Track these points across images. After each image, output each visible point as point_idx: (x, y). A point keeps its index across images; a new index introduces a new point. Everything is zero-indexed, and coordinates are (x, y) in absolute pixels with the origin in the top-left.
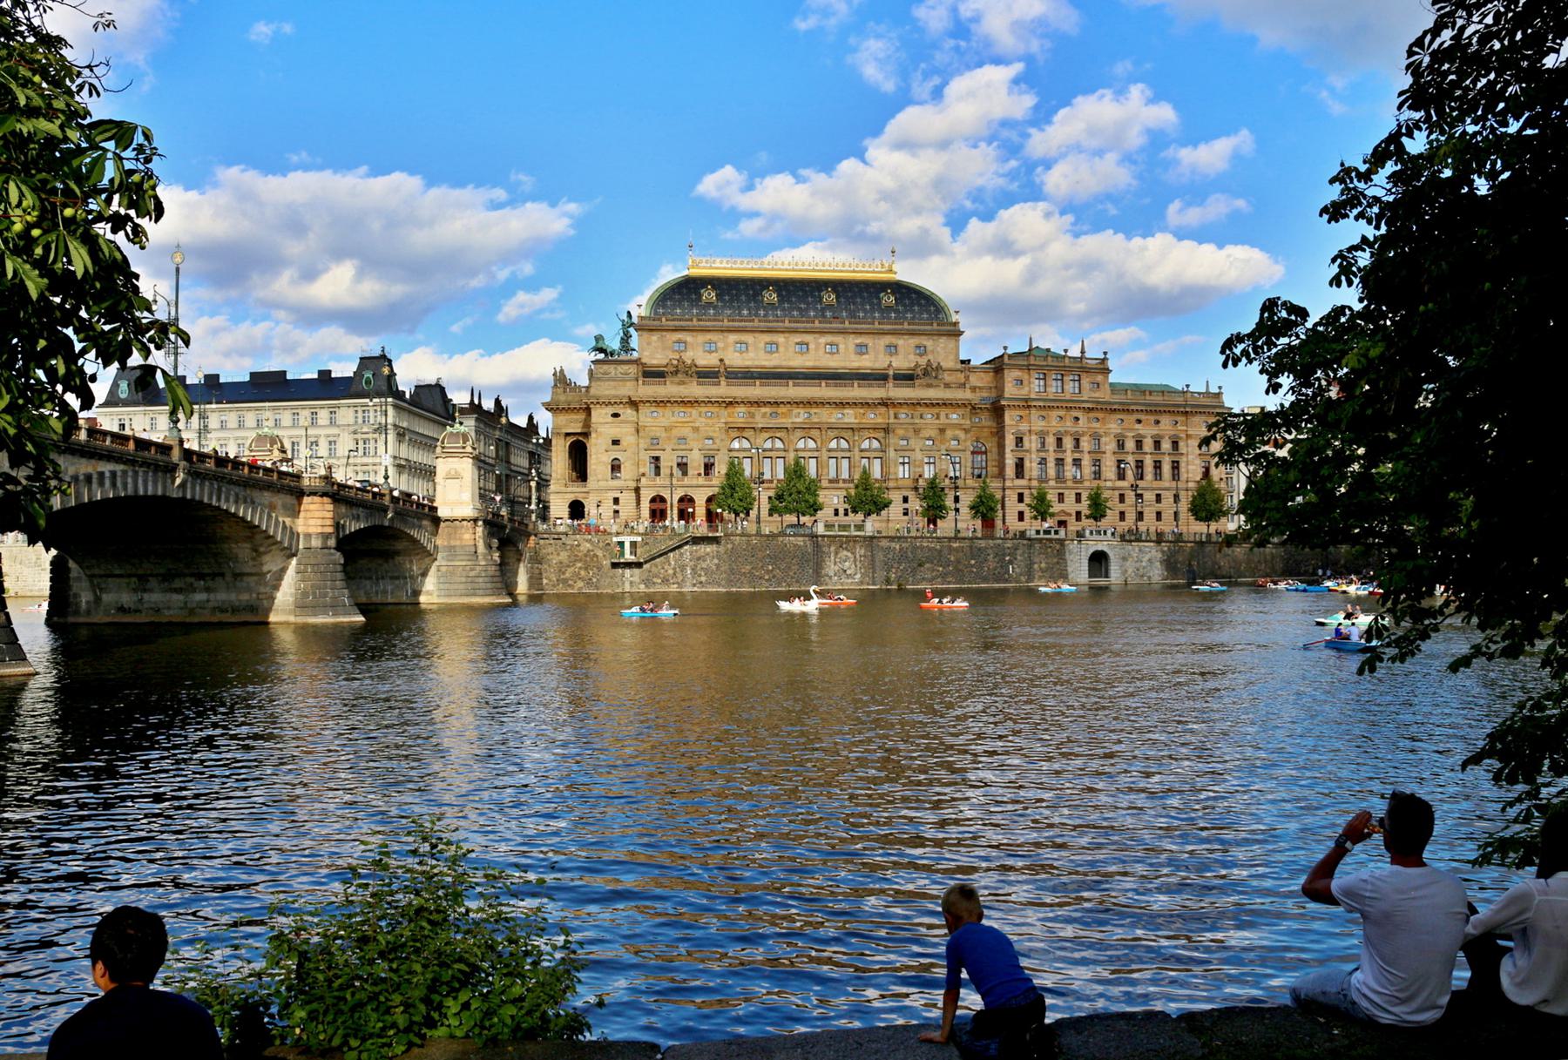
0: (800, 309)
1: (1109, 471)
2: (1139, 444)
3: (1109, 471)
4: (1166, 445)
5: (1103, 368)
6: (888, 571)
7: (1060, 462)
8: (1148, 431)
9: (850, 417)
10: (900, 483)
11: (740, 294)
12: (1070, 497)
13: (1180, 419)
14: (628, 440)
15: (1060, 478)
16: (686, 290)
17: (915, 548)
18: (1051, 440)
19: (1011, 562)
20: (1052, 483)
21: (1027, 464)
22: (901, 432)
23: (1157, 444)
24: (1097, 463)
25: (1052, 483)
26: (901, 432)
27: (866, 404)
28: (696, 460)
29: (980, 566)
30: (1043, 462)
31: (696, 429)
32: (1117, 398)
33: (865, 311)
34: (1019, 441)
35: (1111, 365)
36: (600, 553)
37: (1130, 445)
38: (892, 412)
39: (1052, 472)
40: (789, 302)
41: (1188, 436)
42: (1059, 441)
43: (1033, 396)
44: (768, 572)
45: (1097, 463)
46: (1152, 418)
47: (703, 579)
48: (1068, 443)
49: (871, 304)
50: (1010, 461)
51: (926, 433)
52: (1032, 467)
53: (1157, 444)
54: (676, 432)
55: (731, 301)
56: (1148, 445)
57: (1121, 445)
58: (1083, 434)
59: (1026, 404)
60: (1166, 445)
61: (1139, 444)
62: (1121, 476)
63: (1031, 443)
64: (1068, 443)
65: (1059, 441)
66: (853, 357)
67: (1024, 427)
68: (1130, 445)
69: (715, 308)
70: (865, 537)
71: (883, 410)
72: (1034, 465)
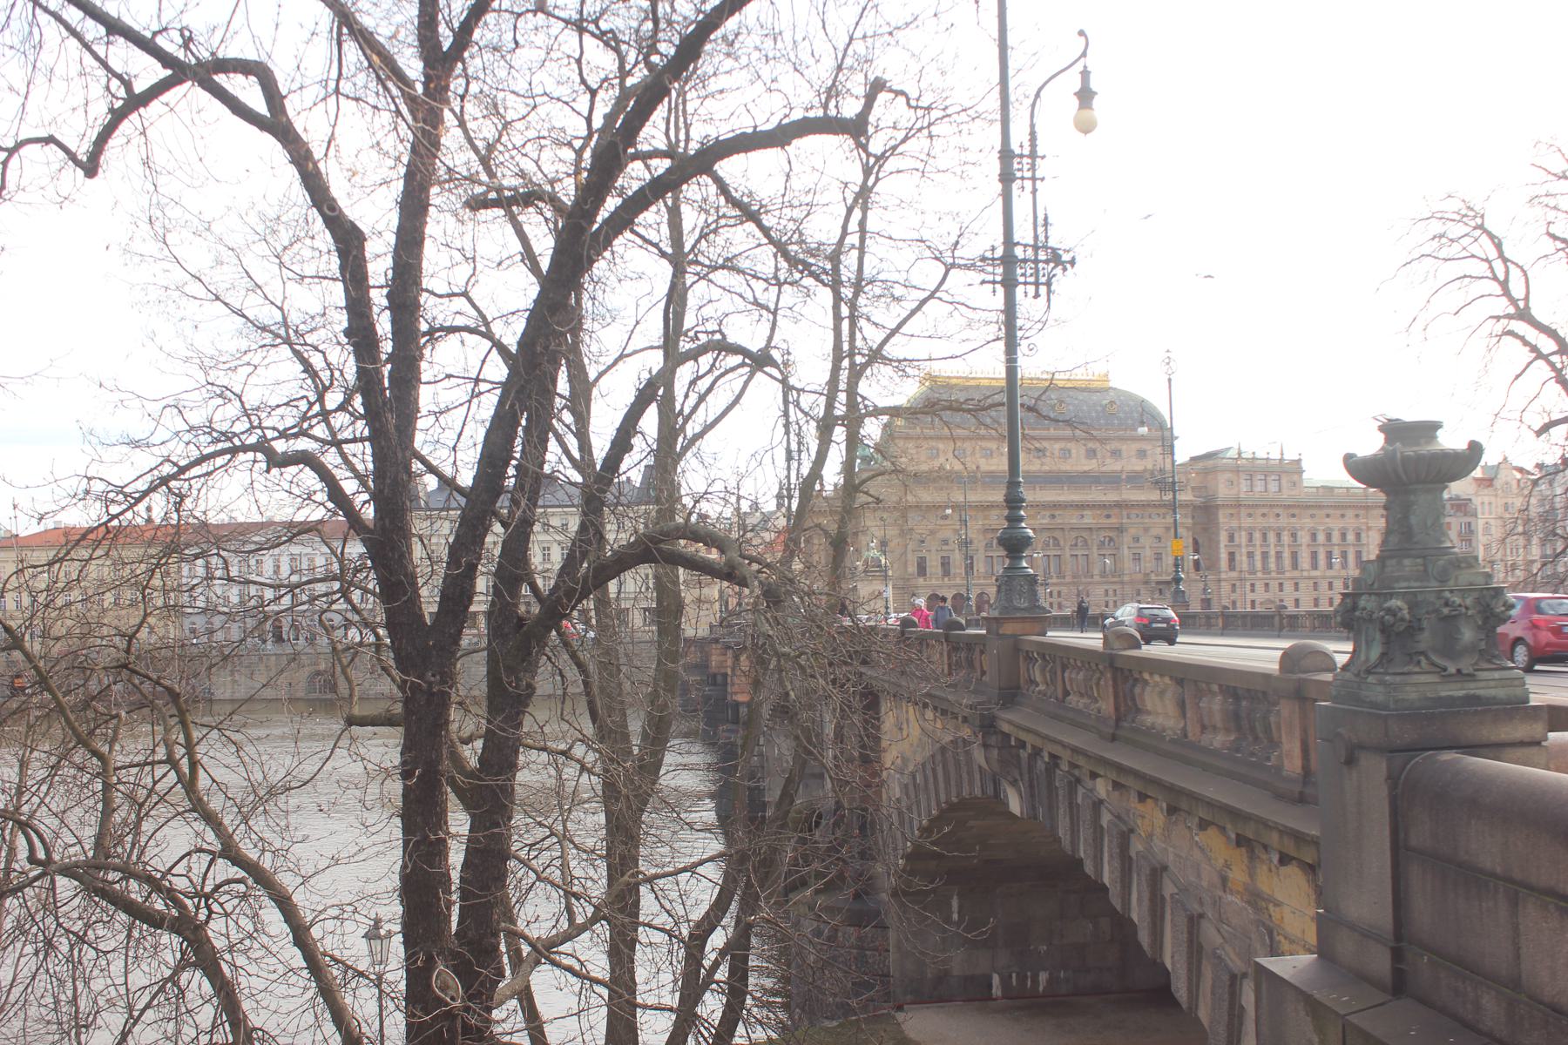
1: (1305, 562)
2: (1329, 537)
3: (1305, 562)
4: (1351, 537)
5: (1296, 468)
7: (1265, 555)
8: (1335, 524)
9: (1089, 519)
12: (1274, 585)
13: (1361, 512)
15: (1265, 569)
18: (1257, 535)
20: (1259, 575)
21: (1237, 557)
22: (1133, 531)
23: (1343, 536)
24: (1294, 556)
25: (1259, 575)
26: (1133, 531)
27: (1103, 506)
30: (1250, 555)
34: (1231, 538)
35: (1304, 465)
37: (1321, 538)
38: (1125, 513)
39: (1259, 565)
41: (1369, 529)
42: (1265, 536)
46: (1339, 512)
48: (1272, 537)
50: (1224, 556)
51: (1154, 532)
52: (1242, 560)
53: (1343, 536)
56: (1336, 538)
57: (1314, 536)
59: (1237, 505)
60: (1351, 537)
61: (1329, 537)
62: (1315, 566)
63: (1242, 538)
64: (1272, 537)
65: (1265, 536)
66: (1084, 461)
67: (1234, 524)
68: (1321, 538)
71: (1116, 511)
72: (1244, 558)
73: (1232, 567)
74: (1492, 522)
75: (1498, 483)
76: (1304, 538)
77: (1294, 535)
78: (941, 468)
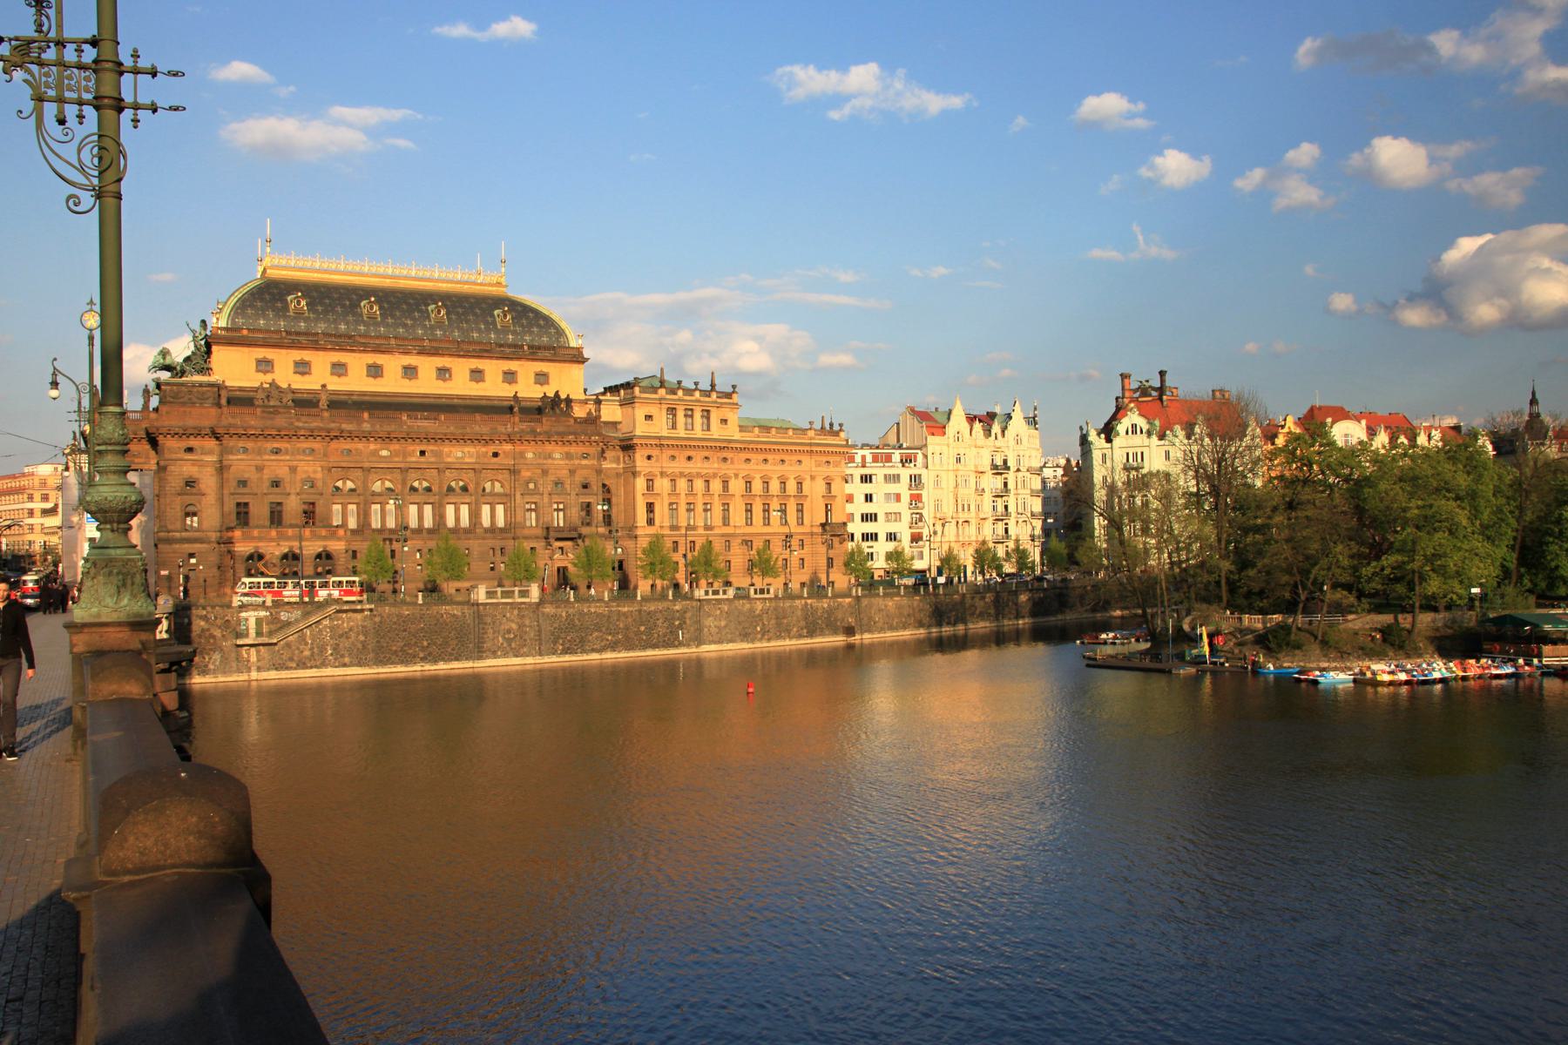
0: (405, 326)
1: (738, 517)
6: (555, 643)
10: (526, 532)
11: (333, 300)
14: (208, 481)
16: (270, 294)
17: (582, 614)
19: (680, 627)
26: (526, 474)
28: (293, 506)
29: (650, 630)
31: (293, 470)
32: (748, 437)
33: (479, 331)
36: (218, 633)
40: (393, 316)
41: (813, 478)
43: (665, 433)
44: (423, 649)
45: (726, 508)
47: (347, 660)
49: (486, 323)
54: (267, 475)
55: (326, 312)
58: (715, 476)
59: (660, 443)
60: (792, 487)
63: (662, 485)
69: (306, 320)
70: (530, 604)
73: (650, 522)
74: (943, 475)
75: (951, 428)
76: (737, 486)
77: (725, 483)
78: (273, 384)
